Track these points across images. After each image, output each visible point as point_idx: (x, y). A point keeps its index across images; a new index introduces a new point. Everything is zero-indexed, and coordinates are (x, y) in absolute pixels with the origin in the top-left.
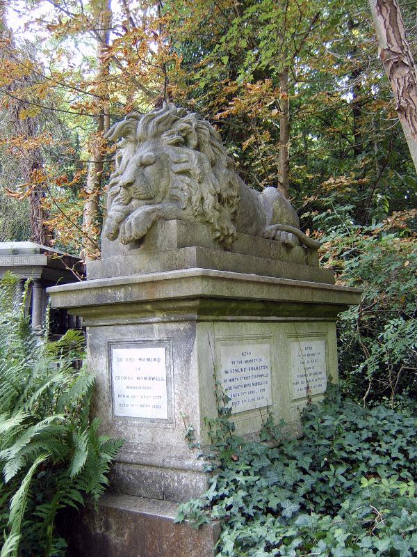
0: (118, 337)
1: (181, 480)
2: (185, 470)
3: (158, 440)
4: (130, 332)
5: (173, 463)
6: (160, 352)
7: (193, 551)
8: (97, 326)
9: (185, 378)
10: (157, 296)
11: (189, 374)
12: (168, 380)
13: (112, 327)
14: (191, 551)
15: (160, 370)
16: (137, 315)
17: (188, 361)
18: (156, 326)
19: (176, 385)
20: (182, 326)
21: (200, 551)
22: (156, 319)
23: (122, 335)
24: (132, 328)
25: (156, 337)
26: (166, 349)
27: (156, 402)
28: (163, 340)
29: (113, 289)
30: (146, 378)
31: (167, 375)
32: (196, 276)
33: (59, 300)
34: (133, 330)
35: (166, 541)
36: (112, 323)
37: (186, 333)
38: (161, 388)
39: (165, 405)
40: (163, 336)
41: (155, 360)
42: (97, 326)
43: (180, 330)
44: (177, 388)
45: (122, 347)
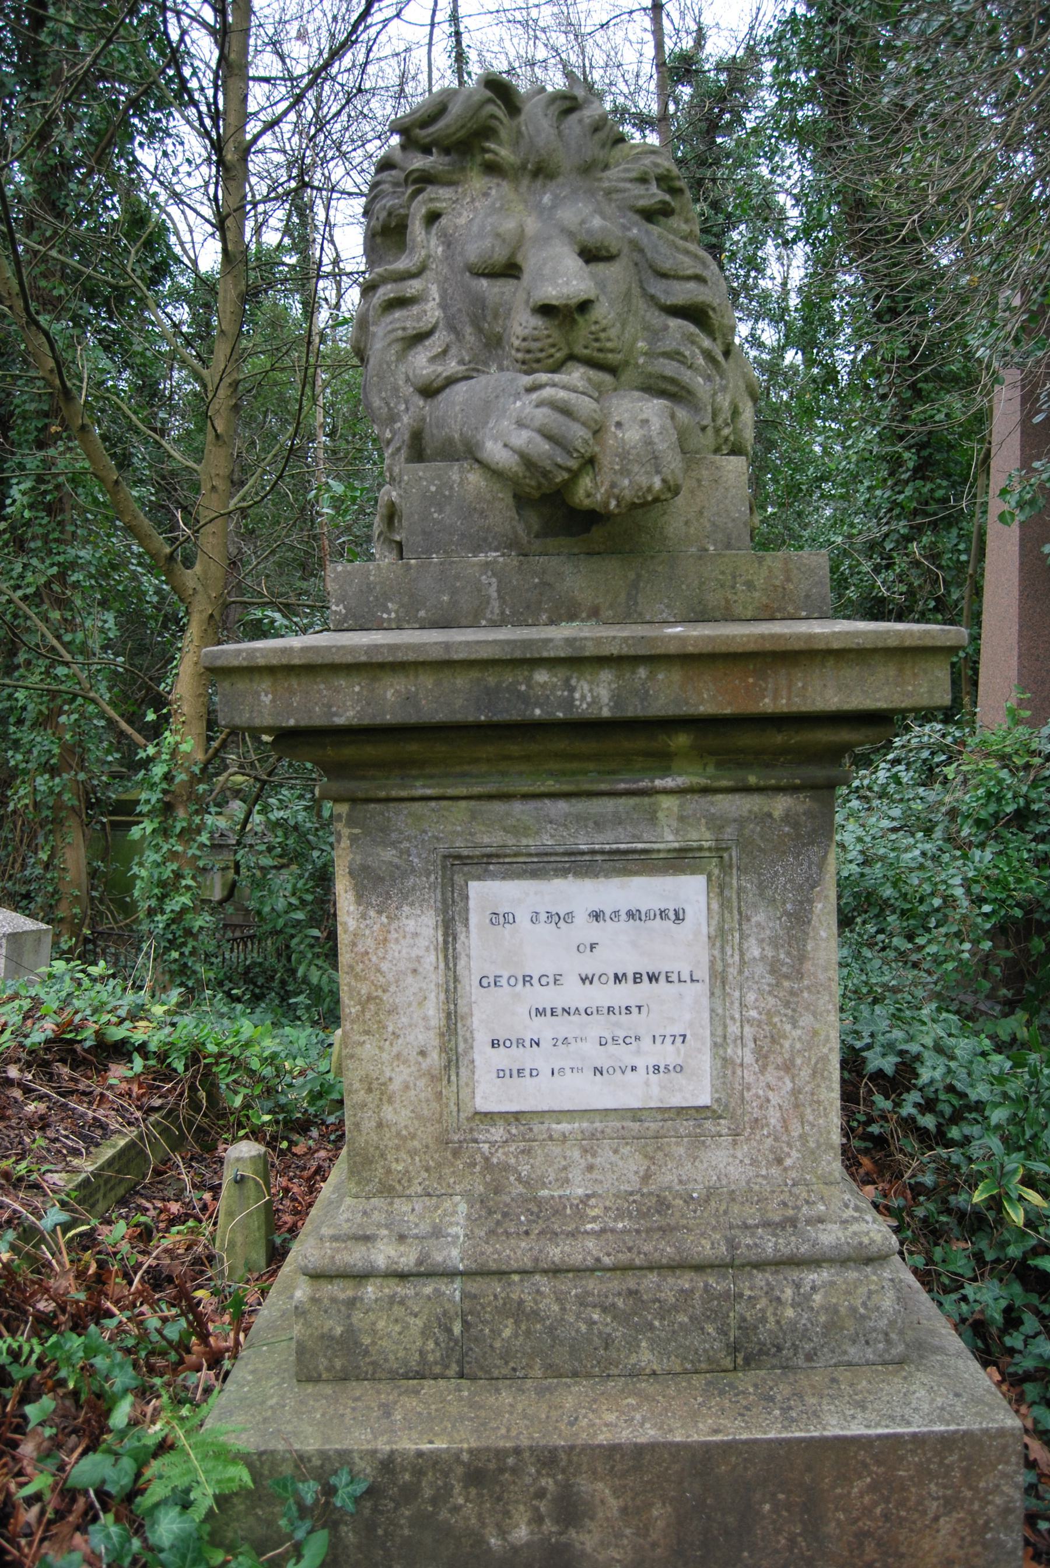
0: (491, 839)
1: (808, 1298)
2: (814, 1262)
3: (667, 1177)
4: (553, 822)
5: (770, 1245)
6: (691, 891)
7: (942, 1520)
8: (388, 800)
9: (789, 970)
10: (767, 705)
11: (802, 958)
12: (719, 978)
13: (463, 804)
14: (936, 1519)
15: (686, 947)
16: (591, 766)
17: (799, 919)
18: (668, 803)
19: (751, 997)
20: (780, 805)
21: (970, 1512)
22: (669, 782)
23: (514, 831)
24: (562, 805)
25: (669, 839)
26: (709, 880)
27: (669, 1054)
28: (700, 849)
29: (562, 672)
30: (637, 978)
31: (712, 963)
32: (423, 664)
33: (267, 699)
34: (567, 816)
35: (837, 1509)
36: (463, 791)
37: (796, 825)
38: (686, 1007)
39: (704, 1062)
40: (701, 836)
41: (663, 914)
42: (388, 800)
43: (770, 815)
44: (755, 999)
45: (506, 876)
